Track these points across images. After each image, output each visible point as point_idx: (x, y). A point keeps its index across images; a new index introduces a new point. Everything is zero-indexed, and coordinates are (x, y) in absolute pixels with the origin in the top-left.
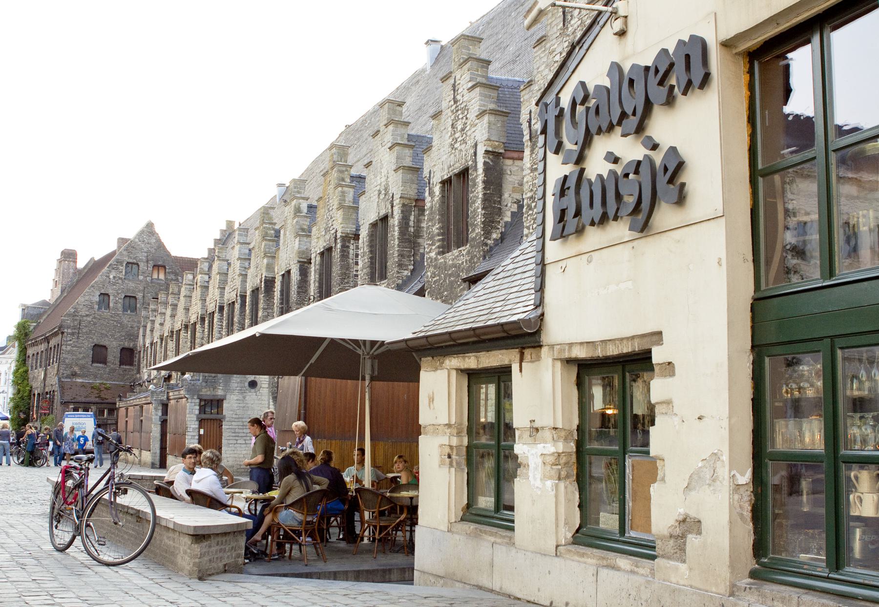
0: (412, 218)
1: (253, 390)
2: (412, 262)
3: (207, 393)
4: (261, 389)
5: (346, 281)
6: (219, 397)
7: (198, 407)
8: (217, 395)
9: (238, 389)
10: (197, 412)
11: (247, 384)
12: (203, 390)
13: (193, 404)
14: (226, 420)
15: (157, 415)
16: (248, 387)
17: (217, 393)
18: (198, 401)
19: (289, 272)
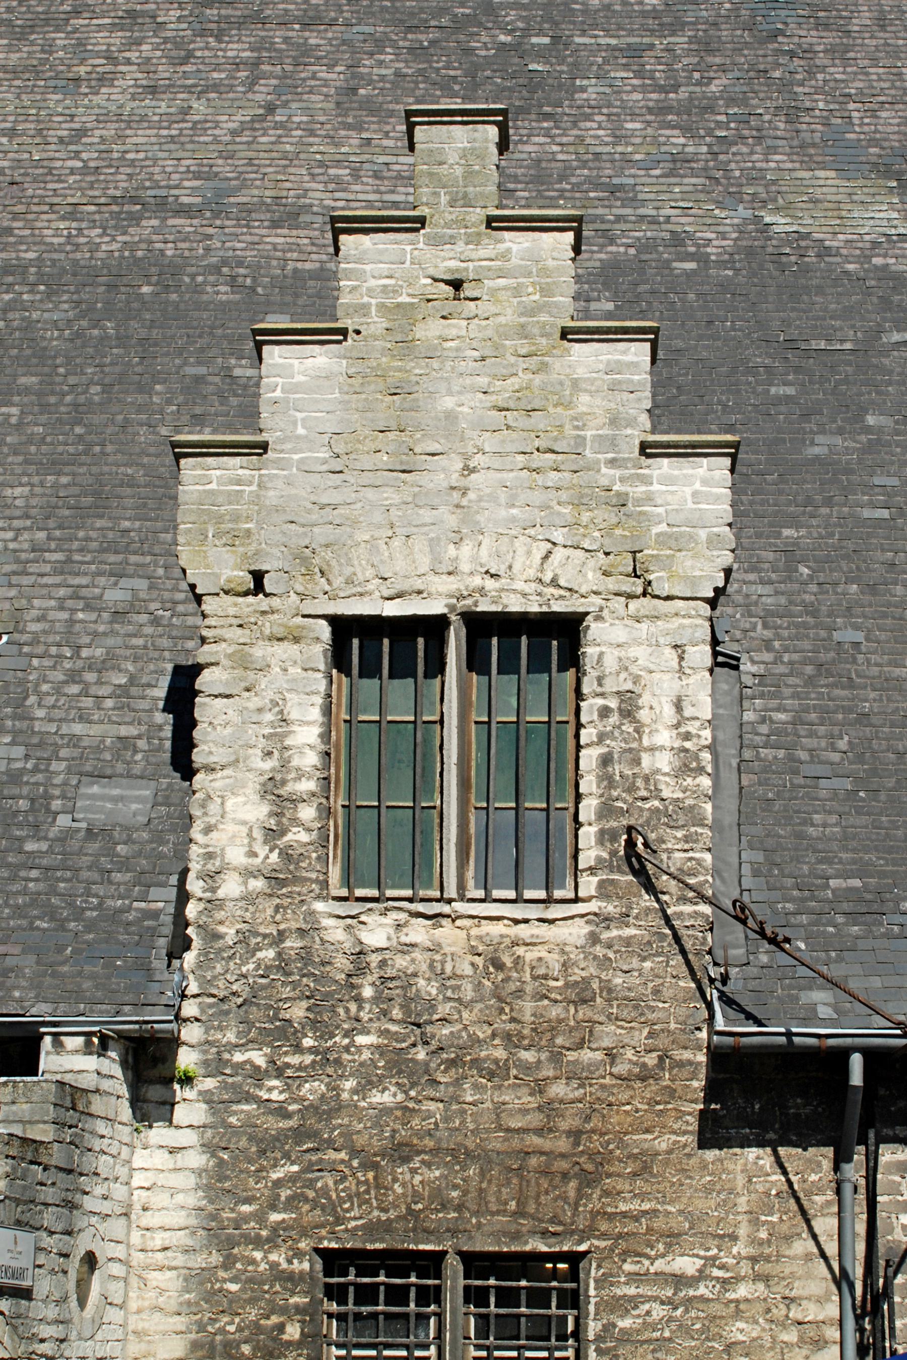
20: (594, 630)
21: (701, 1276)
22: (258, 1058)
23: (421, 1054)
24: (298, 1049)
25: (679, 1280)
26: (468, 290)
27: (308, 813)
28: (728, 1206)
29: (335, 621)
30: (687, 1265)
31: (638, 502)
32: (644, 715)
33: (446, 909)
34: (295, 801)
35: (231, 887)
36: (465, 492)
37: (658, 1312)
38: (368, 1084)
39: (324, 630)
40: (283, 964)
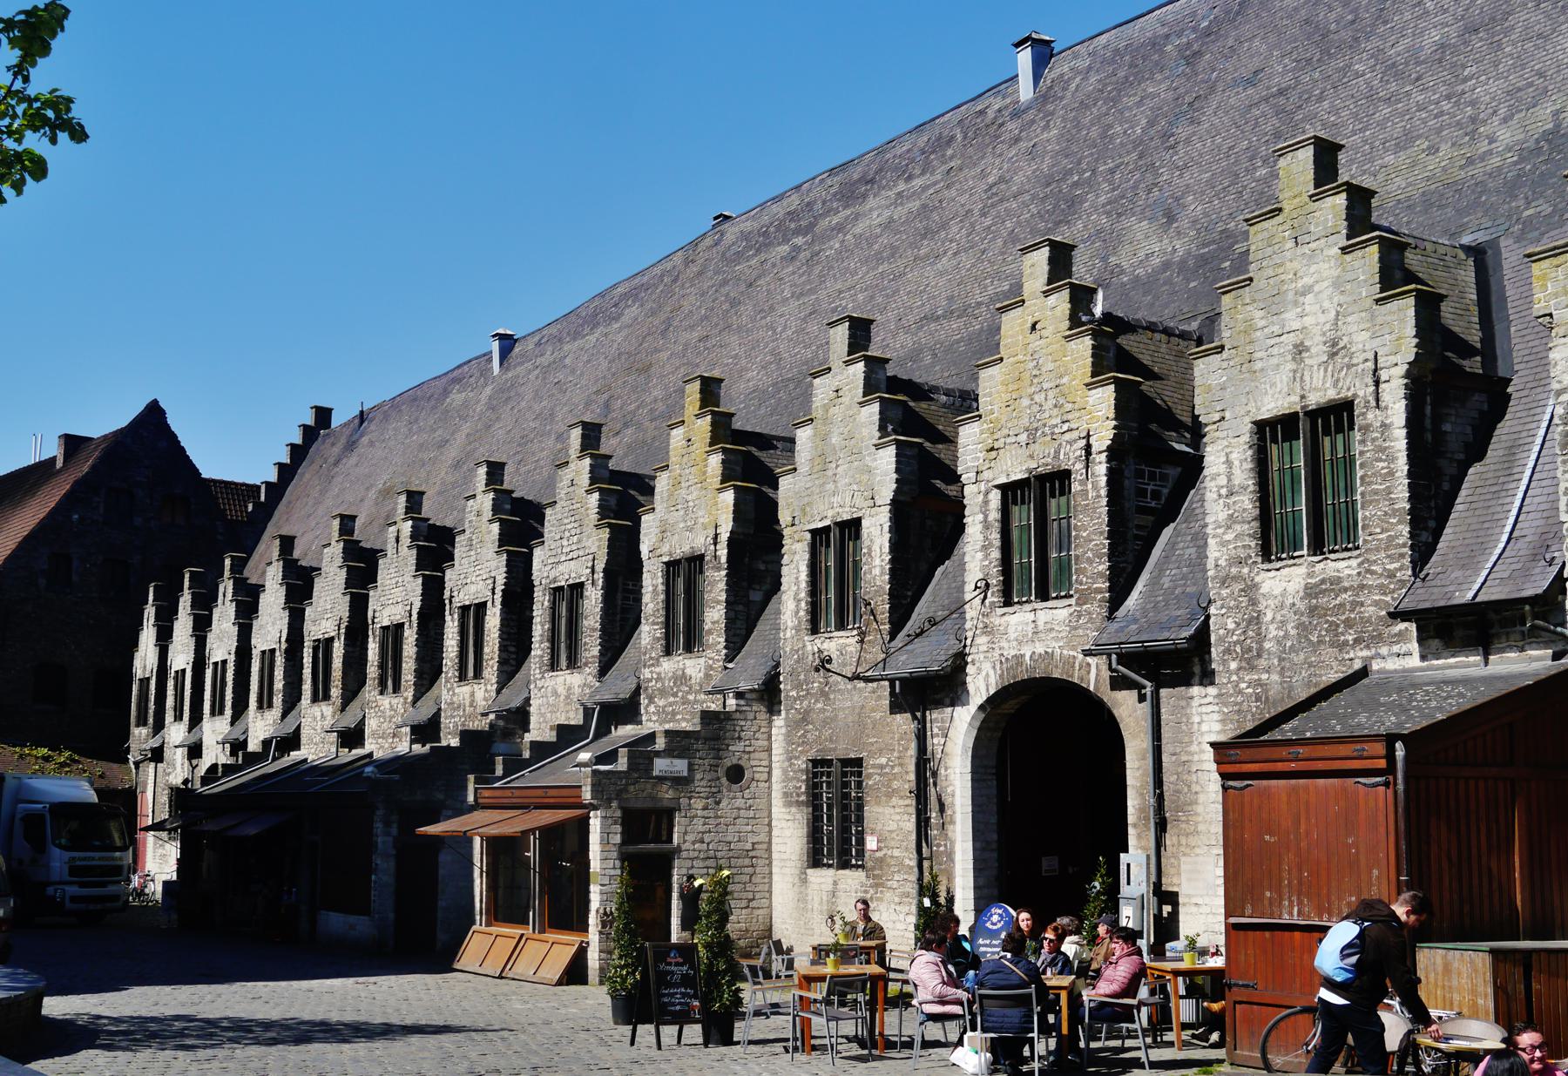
0: (1428, 410)
1: (735, 787)
2: (1434, 512)
3: (639, 796)
4: (754, 784)
5: (1120, 549)
6: (666, 804)
7: (619, 828)
8: (661, 799)
9: (703, 783)
10: (617, 839)
11: (721, 772)
12: (631, 788)
13: (610, 821)
14: (684, 854)
15: (388, 834)
16: (724, 780)
17: (660, 795)
18: (619, 813)
19: (852, 528)
20: (864, 522)
21: (887, 765)
22: (794, 693)
23: (827, 689)
24: (803, 690)
25: (882, 767)
26: (840, 394)
27: (803, 604)
28: (893, 738)
29: (811, 531)
30: (883, 761)
31: (874, 469)
32: (873, 554)
33: (832, 635)
34: (799, 600)
35: (788, 635)
36: (835, 475)
37: (878, 778)
38: (817, 701)
39: (808, 536)
40: (798, 661)
